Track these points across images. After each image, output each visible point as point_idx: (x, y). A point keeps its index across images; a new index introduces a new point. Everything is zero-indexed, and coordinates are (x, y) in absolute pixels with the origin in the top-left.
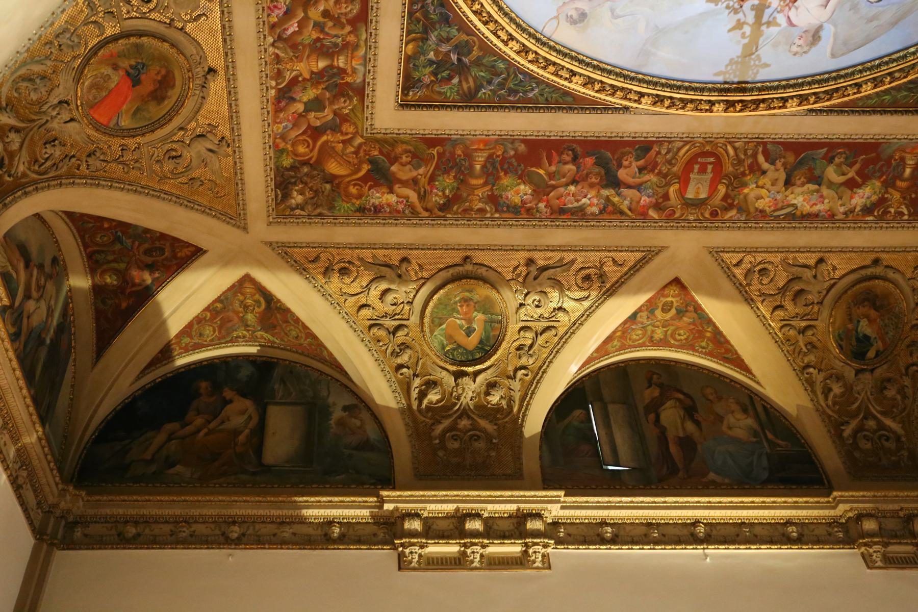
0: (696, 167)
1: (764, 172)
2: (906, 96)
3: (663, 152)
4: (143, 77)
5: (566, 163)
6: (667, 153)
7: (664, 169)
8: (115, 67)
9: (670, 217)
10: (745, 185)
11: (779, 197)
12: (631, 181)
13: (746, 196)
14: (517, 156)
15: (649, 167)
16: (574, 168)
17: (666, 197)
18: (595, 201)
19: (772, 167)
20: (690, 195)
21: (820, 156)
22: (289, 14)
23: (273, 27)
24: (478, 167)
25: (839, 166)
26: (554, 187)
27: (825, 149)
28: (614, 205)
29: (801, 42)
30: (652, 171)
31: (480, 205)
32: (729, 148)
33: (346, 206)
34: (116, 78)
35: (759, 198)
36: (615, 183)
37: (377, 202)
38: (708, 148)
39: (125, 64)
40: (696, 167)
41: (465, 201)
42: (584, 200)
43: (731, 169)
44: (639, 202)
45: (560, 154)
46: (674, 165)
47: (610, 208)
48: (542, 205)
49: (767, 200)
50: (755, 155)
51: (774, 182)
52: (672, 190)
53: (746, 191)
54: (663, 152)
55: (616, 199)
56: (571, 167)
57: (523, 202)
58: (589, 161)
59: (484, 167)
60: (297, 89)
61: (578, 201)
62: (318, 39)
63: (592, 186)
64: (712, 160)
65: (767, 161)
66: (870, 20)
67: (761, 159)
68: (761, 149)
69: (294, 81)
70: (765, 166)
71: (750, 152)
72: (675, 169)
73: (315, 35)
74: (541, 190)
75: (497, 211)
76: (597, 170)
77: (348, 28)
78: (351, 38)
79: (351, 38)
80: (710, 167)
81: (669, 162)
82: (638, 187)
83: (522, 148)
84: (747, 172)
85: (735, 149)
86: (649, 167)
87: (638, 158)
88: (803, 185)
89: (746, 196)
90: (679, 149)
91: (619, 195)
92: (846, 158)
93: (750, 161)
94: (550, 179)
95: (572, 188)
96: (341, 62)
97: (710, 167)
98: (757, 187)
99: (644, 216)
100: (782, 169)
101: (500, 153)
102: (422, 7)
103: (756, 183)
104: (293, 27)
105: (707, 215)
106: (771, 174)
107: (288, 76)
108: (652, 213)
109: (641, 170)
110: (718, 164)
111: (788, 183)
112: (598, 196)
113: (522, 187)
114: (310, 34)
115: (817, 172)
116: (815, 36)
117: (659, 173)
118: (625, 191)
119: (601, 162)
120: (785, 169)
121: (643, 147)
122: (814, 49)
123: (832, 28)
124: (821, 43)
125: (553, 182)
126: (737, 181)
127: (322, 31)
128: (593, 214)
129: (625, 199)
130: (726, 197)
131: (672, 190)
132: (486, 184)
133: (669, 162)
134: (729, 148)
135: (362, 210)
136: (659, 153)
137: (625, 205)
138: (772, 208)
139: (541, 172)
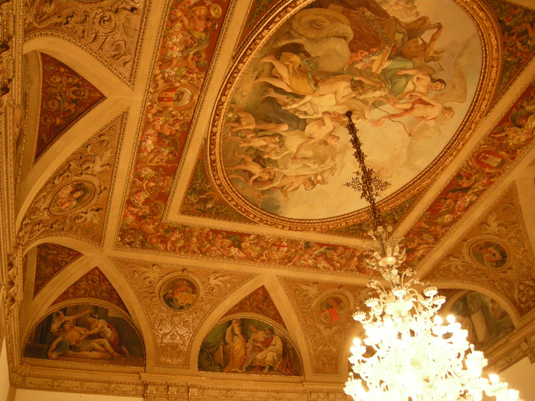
0: (483, 160)
1: (507, 135)
2: (511, 72)
3: (465, 170)
4: (331, 305)
5: (445, 202)
6: (467, 169)
7: (474, 171)
8: (324, 311)
9: (500, 174)
10: (507, 144)
11: (525, 131)
12: (471, 183)
13: (513, 144)
14: (430, 215)
15: (469, 176)
16: (449, 200)
17: (489, 173)
18: (471, 197)
19: (506, 132)
20: (495, 165)
21: (516, 111)
22: (333, 265)
23: (335, 270)
24: (427, 226)
25: (528, 104)
26: (454, 208)
27: (514, 109)
28: (478, 191)
29: (447, 115)
30: (471, 175)
31: (444, 230)
32: (482, 147)
33: (415, 262)
34: (327, 312)
35: (519, 140)
36: (468, 188)
37: (420, 255)
38: (476, 155)
39: (324, 308)
40: (483, 160)
41: (438, 233)
42: (468, 200)
43: (494, 148)
44: (483, 183)
45: (440, 202)
46: (475, 168)
47: (479, 193)
48: (459, 213)
49: (523, 136)
50: (494, 138)
51: (516, 132)
52: (487, 170)
53: (511, 144)
54: (465, 170)
55: (476, 190)
56: (448, 201)
57: (453, 218)
58: (450, 194)
59: (428, 225)
60: (360, 266)
61: (466, 202)
62: (346, 259)
63: (463, 196)
64: (483, 154)
65: (500, 133)
66: (454, 87)
67: (498, 136)
68: (493, 135)
69: (357, 267)
70: (503, 134)
71: (491, 139)
72: (477, 168)
73: (344, 259)
74: (452, 211)
75: (450, 226)
76: (456, 193)
77: (347, 251)
78: (351, 251)
79: (351, 251)
80: (487, 155)
81: (472, 169)
82: (476, 181)
83: (428, 213)
84: (501, 142)
85: (485, 145)
86: (469, 176)
87: (462, 179)
88: (527, 121)
89: (513, 144)
90: (468, 164)
91: (474, 188)
92: (526, 100)
93: (495, 141)
94: (449, 207)
95: (458, 203)
96: (358, 254)
97: (487, 155)
98: (512, 139)
99: (491, 183)
100: (511, 128)
101: (425, 219)
102: (352, 230)
103: (510, 139)
104: (338, 265)
105: (511, 161)
106: (509, 133)
107: (354, 268)
108: (492, 180)
109: (468, 179)
110: (488, 152)
111: (520, 127)
112: (469, 195)
113: (446, 217)
114: (343, 261)
115: (525, 114)
116: (448, 109)
117: (475, 174)
118: (474, 186)
119: (453, 191)
120: (511, 127)
121: (459, 176)
122: (454, 110)
123: (449, 103)
124: (453, 106)
125: (451, 208)
126: (502, 146)
127: (343, 258)
128: (476, 199)
129: (479, 187)
130: (508, 152)
131: (487, 170)
132: (436, 226)
133: (472, 169)
134: (482, 147)
135: (420, 260)
136: (465, 172)
137: (481, 188)
138: (530, 135)
139: (444, 210)
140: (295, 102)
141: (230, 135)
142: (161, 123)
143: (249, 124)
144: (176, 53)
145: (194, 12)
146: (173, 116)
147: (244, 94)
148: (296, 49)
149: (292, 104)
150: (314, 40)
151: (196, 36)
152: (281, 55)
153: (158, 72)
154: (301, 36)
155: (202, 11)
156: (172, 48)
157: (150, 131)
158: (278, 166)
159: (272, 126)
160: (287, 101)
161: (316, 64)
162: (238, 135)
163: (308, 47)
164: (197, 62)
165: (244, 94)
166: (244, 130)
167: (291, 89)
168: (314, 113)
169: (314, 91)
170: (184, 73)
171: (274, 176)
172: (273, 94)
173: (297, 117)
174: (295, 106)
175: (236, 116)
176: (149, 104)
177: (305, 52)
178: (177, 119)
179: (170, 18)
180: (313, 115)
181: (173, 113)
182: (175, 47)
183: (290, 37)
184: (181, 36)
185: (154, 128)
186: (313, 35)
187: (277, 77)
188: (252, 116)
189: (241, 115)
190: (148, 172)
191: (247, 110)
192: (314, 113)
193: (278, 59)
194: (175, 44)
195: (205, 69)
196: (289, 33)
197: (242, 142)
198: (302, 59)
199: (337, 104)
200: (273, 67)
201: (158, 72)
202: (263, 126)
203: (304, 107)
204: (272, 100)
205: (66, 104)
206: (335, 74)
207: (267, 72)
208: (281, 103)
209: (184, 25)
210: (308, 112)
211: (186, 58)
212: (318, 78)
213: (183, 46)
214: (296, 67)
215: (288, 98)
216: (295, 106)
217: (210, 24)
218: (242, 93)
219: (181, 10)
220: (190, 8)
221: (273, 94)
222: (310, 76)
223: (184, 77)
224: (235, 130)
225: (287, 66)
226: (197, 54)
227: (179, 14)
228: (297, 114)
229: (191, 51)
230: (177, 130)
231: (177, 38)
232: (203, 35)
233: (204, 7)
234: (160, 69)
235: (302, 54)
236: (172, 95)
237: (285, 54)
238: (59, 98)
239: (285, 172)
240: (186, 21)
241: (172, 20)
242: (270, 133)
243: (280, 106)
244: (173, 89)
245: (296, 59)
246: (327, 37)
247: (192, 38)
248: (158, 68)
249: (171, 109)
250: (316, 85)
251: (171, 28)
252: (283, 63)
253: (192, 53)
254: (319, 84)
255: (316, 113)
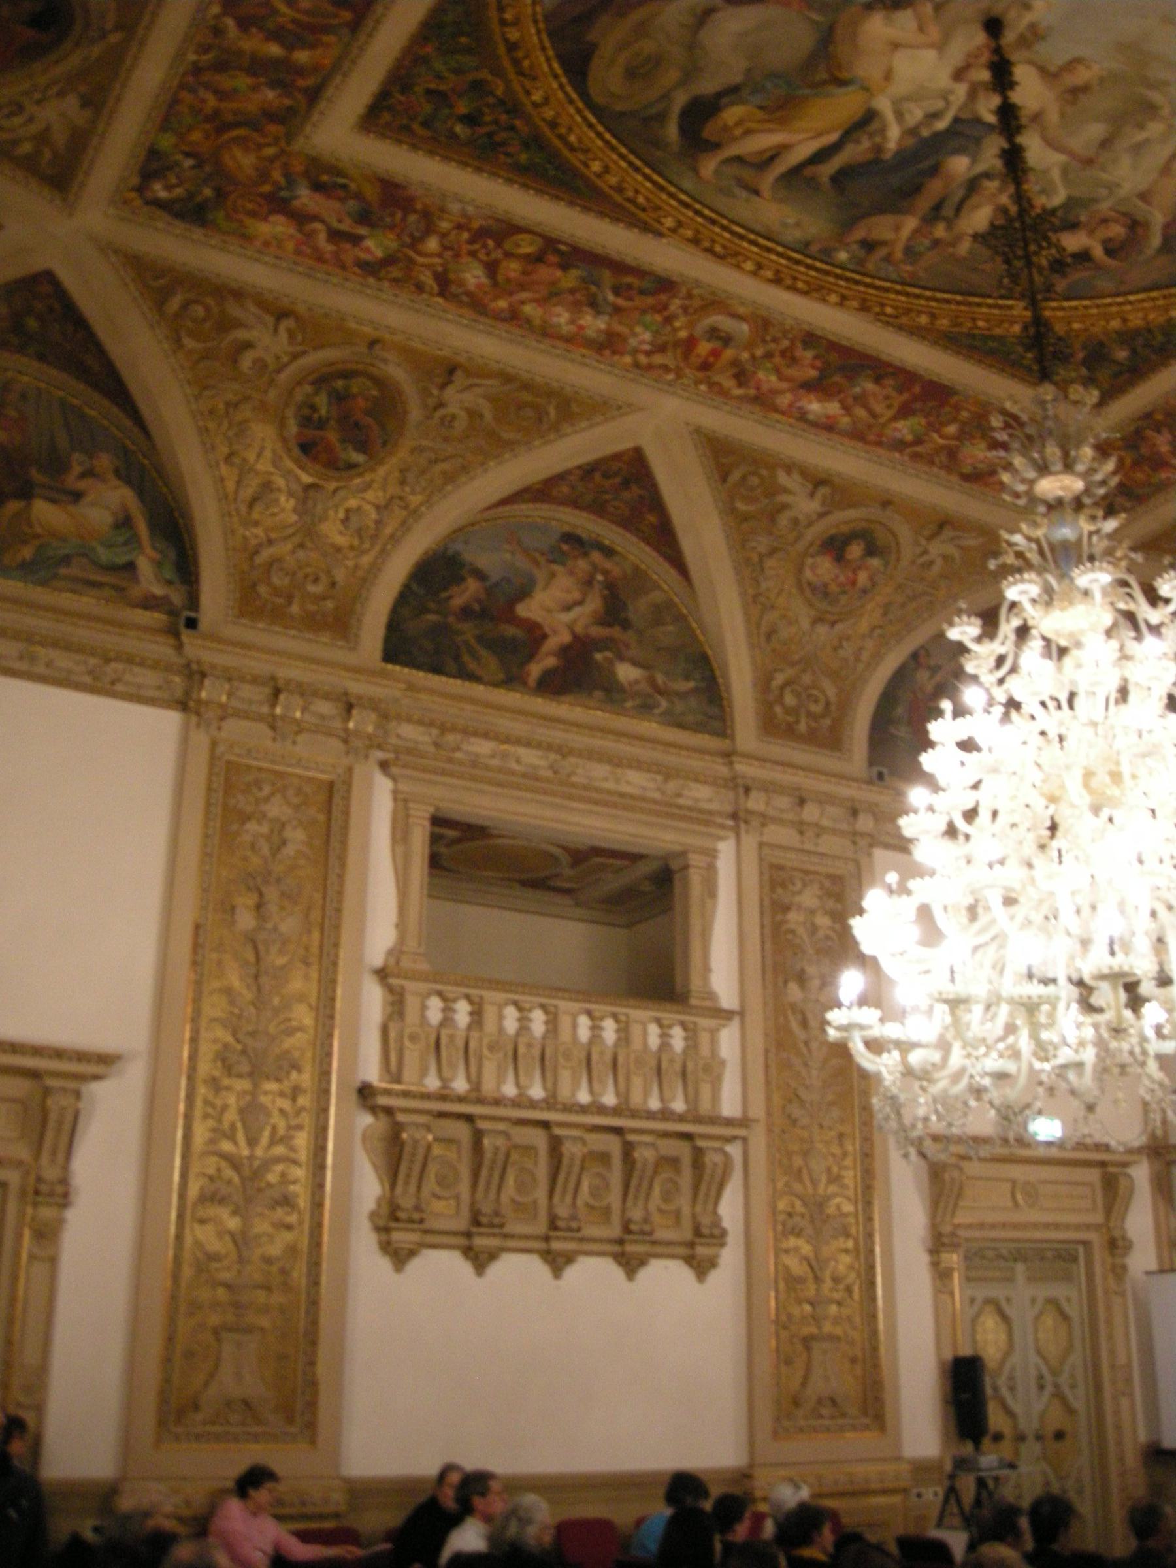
140: (883, 131)
141: (909, 268)
142: (773, 378)
143: (897, 229)
144: (594, 324)
145: (508, 280)
146: (769, 356)
147: (791, 221)
148: (701, 112)
149: (884, 137)
150: (689, 74)
151: (570, 285)
152: (707, 141)
153: (628, 359)
154: (666, 97)
155: (512, 268)
156: (581, 328)
157: (784, 400)
158: (1095, 200)
159: (935, 187)
160: (866, 144)
161: (774, 75)
162: (920, 254)
163: (708, 86)
164: (642, 292)
165: (791, 221)
166: (909, 239)
167: (828, 132)
168: (946, 99)
169: (866, 89)
170: (658, 318)
171: (1125, 214)
172: (827, 170)
173: (937, 135)
174: (894, 133)
175: (855, 247)
176: (703, 388)
177: (719, 95)
178: (783, 354)
179: (504, 320)
180: (948, 102)
181: (759, 352)
182: (582, 322)
183: (661, 117)
184: (558, 309)
185: (775, 392)
186: (673, 75)
187: (772, 158)
188: (874, 220)
189: (859, 233)
190: (904, 429)
191: (849, 224)
192: (946, 99)
193: (717, 146)
194: (572, 322)
195: (665, 285)
196: (646, 121)
197: (950, 250)
198: (742, 102)
199: (940, 47)
200: (739, 160)
201: (628, 359)
202: (924, 203)
203: (907, 116)
204: (840, 179)
205: (626, 495)
206: (826, 39)
207: (746, 174)
208: (870, 156)
209: (536, 301)
210: (932, 109)
211: (617, 310)
212: (822, 75)
213: (587, 309)
214: (760, 115)
215: (858, 142)
216: (894, 133)
217: (553, 259)
218: (785, 225)
219: (496, 298)
220: (495, 284)
221: (827, 170)
222: (807, 91)
223: (668, 320)
224: (899, 254)
225: (748, 132)
226: (617, 291)
227: (502, 304)
228: (925, 133)
229: (605, 299)
230: (816, 357)
231: (558, 315)
232: (575, 273)
233: (504, 264)
234: (622, 354)
235: (725, 100)
236: (704, 348)
237: (709, 131)
238: (607, 497)
239: (1126, 189)
240: (524, 295)
241: (513, 316)
242: (960, 194)
243: (877, 161)
244: (690, 344)
245: (732, 114)
246: (692, 46)
247: (572, 291)
248: (616, 358)
249: (745, 356)
250: (842, 83)
251: (528, 321)
252: (734, 139)
253: (611, 297)
254: (845, 75)
255: (945, 96)
